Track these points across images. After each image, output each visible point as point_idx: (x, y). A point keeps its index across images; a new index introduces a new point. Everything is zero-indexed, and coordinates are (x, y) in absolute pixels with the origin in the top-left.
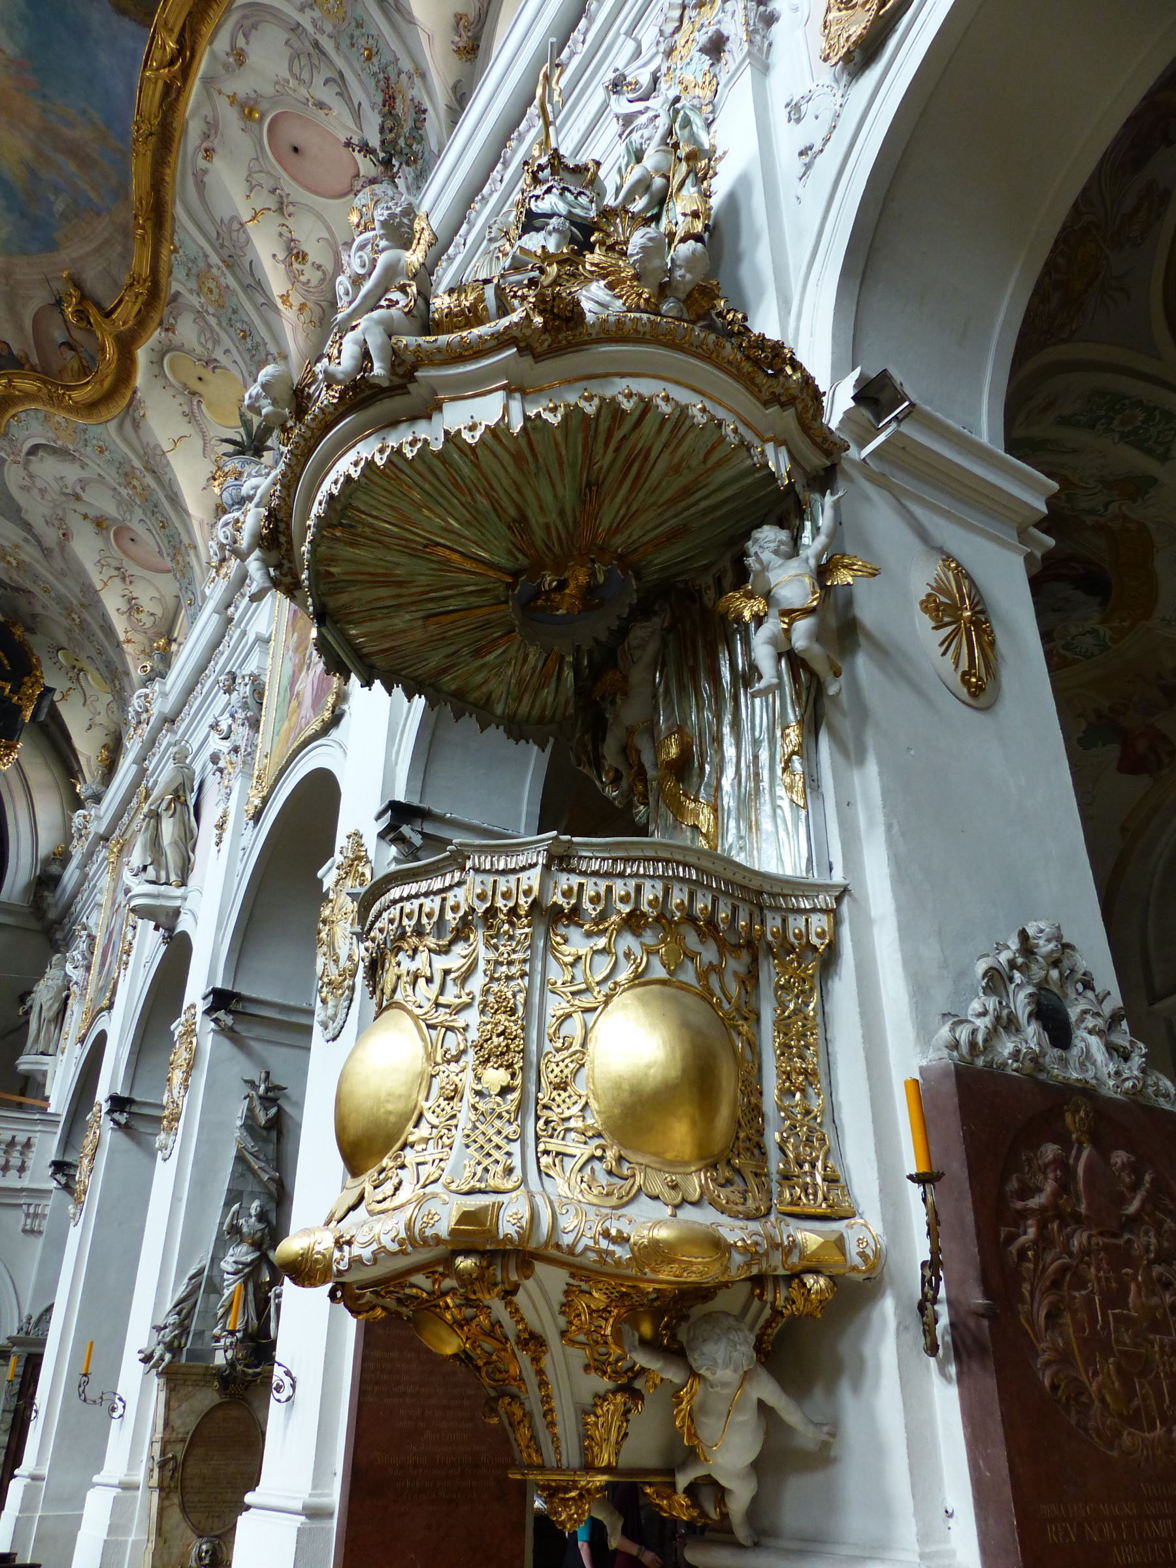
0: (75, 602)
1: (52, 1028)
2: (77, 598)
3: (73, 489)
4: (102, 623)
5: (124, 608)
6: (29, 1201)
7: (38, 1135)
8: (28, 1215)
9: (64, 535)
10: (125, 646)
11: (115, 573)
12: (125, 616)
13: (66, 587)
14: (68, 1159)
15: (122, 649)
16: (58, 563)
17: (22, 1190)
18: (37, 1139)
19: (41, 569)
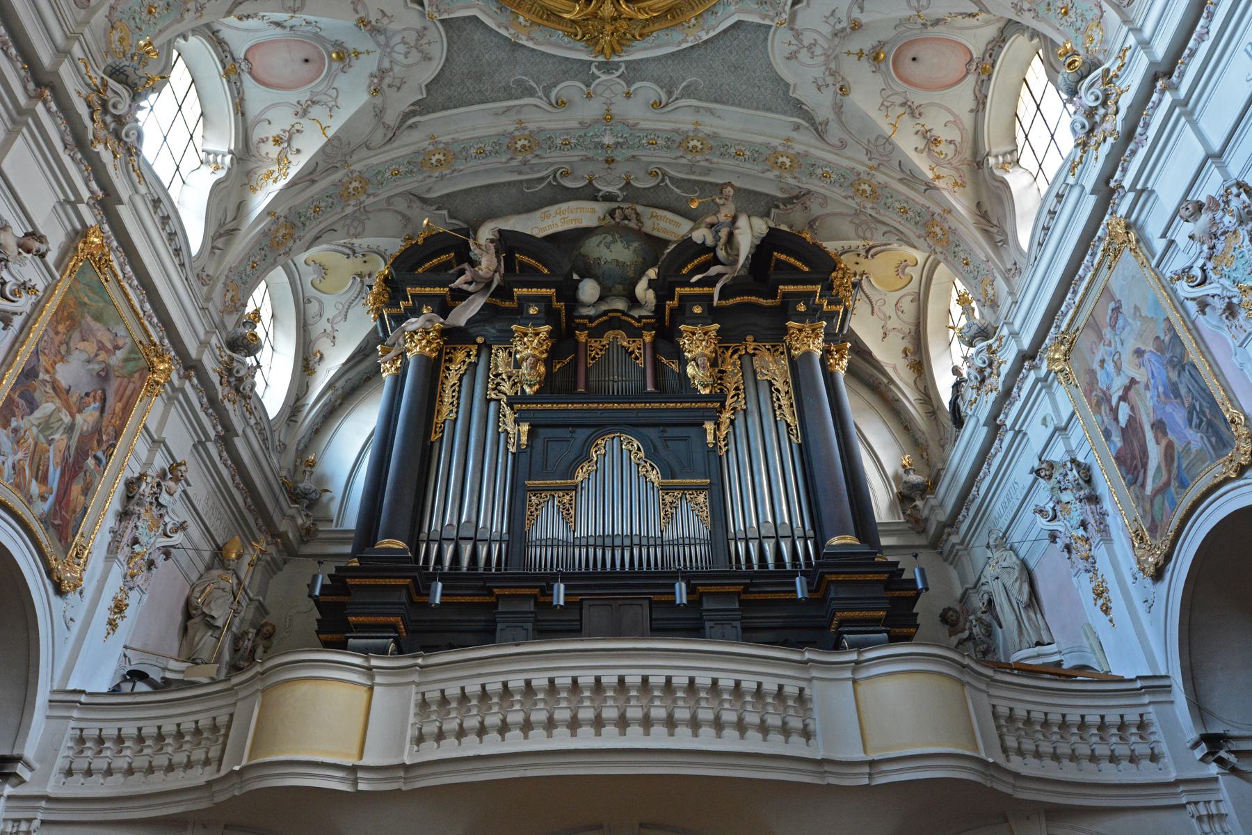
0: (861, 168)
1: (1032, 615)
2: (864, 164)
3: (849, 17)
4: (900, 176)
5: (921, 144)
6: (1194, 798)
7: (1150, 709)
8: (1200, 819)
9: (841, 89)
10: (939, 183)
11: (901, 110)
12: (925, 154)
13: (847, 158)
14: (1218, 729)
15: (938, 189)
16: (835, 133)
17: (1177, 783)
18: (1152, 714)
19: (820, 152)
